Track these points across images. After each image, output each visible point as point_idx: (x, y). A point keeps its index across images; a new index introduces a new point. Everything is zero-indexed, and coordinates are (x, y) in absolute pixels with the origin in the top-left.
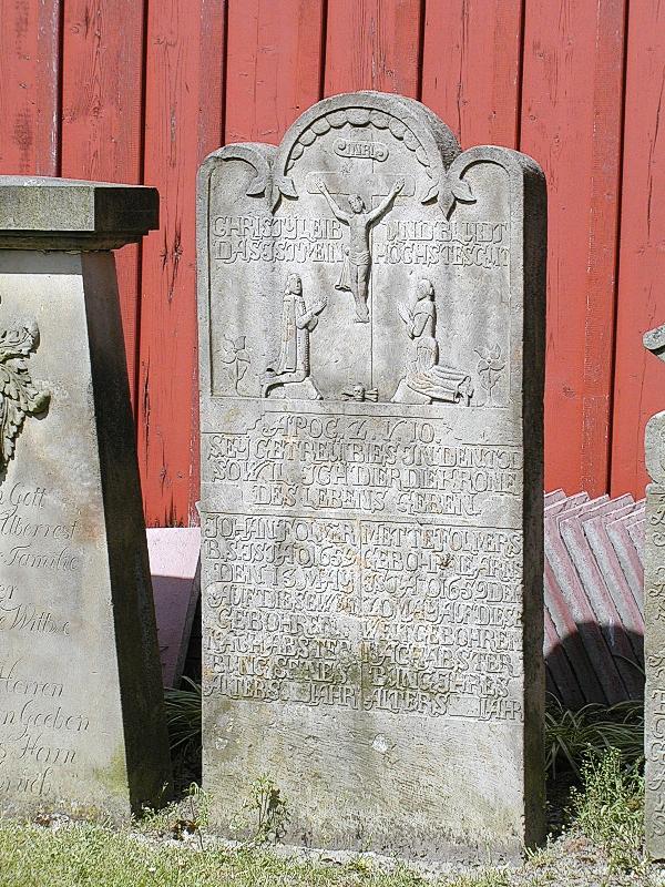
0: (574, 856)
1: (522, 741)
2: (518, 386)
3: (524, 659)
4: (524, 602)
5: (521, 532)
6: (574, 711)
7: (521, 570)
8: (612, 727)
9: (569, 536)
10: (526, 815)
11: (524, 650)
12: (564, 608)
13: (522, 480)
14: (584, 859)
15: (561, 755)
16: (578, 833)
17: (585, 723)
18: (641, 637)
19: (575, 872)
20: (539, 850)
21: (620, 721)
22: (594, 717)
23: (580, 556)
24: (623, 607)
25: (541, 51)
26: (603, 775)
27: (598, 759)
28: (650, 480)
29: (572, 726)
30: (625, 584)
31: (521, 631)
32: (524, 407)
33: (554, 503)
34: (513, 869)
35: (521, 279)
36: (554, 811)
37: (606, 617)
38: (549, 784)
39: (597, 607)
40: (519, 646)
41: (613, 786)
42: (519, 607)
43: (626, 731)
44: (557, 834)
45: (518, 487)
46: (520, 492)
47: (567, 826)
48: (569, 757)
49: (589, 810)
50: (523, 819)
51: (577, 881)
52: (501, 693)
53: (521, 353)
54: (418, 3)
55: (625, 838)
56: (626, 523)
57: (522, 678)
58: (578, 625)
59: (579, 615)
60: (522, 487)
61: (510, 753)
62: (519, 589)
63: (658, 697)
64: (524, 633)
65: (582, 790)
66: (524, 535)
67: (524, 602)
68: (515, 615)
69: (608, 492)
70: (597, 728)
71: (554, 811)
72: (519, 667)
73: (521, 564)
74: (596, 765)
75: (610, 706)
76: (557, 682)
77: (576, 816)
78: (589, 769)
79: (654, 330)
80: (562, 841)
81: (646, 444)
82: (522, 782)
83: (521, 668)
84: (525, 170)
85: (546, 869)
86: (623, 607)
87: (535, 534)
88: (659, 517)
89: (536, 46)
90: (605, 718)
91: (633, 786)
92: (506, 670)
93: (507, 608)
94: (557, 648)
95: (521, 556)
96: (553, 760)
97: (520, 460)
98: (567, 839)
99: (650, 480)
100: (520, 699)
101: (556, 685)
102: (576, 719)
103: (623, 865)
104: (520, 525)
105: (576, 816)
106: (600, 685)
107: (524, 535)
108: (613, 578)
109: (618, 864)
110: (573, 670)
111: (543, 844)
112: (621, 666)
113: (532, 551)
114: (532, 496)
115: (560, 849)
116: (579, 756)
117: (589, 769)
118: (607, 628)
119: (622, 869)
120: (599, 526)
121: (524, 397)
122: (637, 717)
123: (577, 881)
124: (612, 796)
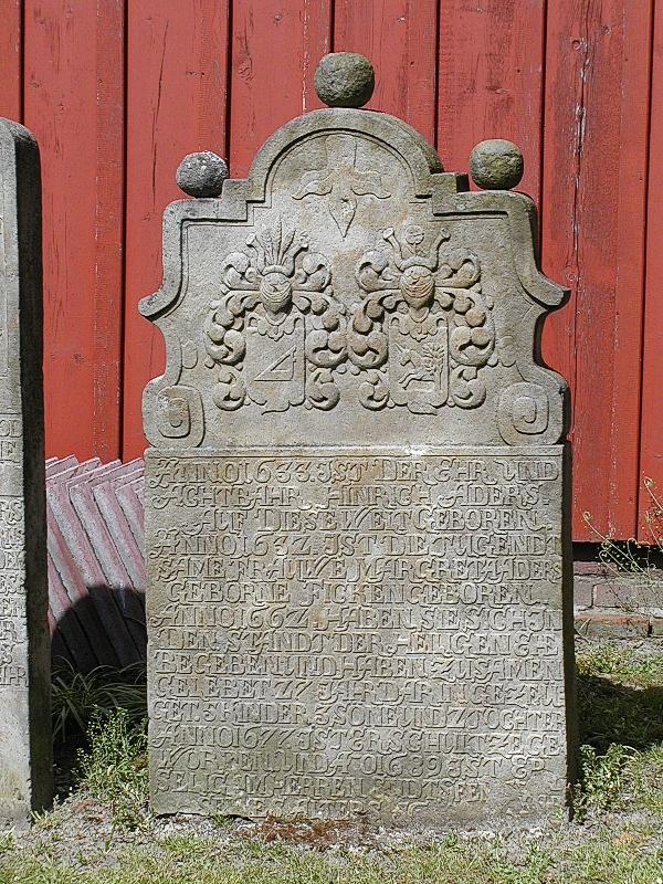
0: (81, 816)
1: (27, 706)
2: (16, 354)
3: (27, 624)
4: (27, 569)
5: (22, 499)
6: (84, 675)
7: (23, 537)
8: (121, 688)
9: (79, 502)
10: (32, 779)
11: (28, 616)
12: (75, 571)
13: (21, 448)
14: (90, 819)
15: (70, 718)
16: (85, 794)
17: (96, 685)
18: (143, 595)
19: (81, 832)
20: (46, 812)
21: (131, 682)
22: (106, 680)
23: (91, 523)
24: (133, 570)
25: (42, 18)
26: (109, 736)
27: (105, 719)
28: (148, 444)
29: (83, 689)
30: (134, 547)
31: (24, 597)
32: (22, 375)
33: (59, 473)
34: (20, 834)
35: (15, 247)
36: (63, 773)
37: (117, 580)
38: (57, 747)
39: (107, 570)
40: (22, 612)
41: (120, 745)
42: (22, 574)
43: (136, 691)
44: (64, 796)
45: (18, 454)
46: (21, 459)
47: (74, 788)
48: (77, 716)
49: (98, 771)
50: (29, 783)
51: (82, 841)
52: (5, 660)
53: (18, 321)
54: (226, 4)
55: (131, 795)
56: (135, 487)
57: (26, 643)
58: (90, 589)
59: (89, 578)
60: (22, 454)
61: (16, 719)
62: (21, 556)
63: (161, 656)
64: (27, 599)
65: (89, 751)
66: (26, 502)
67: (27, 569)
68: (18, 581)
69: (121, 458)
70: (105, 689)
71: (63, 773)
72: (23, 632)
73: (23, 531)
74: (102, 726)
75: (122, 668)
76: (70, 646)
77: (84, 777)
78: (95, 731)
79: (149, 297)
80: (68, 802)
81: (144, 409)
82: (28, 747)
83: (24, 634)
84: (17, 139)
85: (53, 831)
86: (133, 570)
87: (37, 501)
88: (157, 480)
89: (37, 13)
90: (115, 679)
91: (138, 745)
92: (10, 636)
93: (9, 575)
94: (70, 613)
95: (22, 522)
96: (62, 725)
97: (19, 427)
98: (75, 799)
99: (148, 444)
100: (24, 665)
101: (68, 649)
102: (87, 681)
103: (128, 823)
104: (21, 492)
105: (84, 777)
106: (112, 647)
107: (25, 502)
108: (123, 541)
109: (123, 821)
110: (86, 635)
111: (49, 807)
112: (131, 626)
113: (34, 517)
114: (33, 464)
115: (67, 814)
116: (86, 718)
117: (95, 731)
118: (118, 590)
119: (127, 826)
120: (108, 491)
121: (21, 365)
122: (138, 678)
123: (82, 841)
124: (119, 756)
